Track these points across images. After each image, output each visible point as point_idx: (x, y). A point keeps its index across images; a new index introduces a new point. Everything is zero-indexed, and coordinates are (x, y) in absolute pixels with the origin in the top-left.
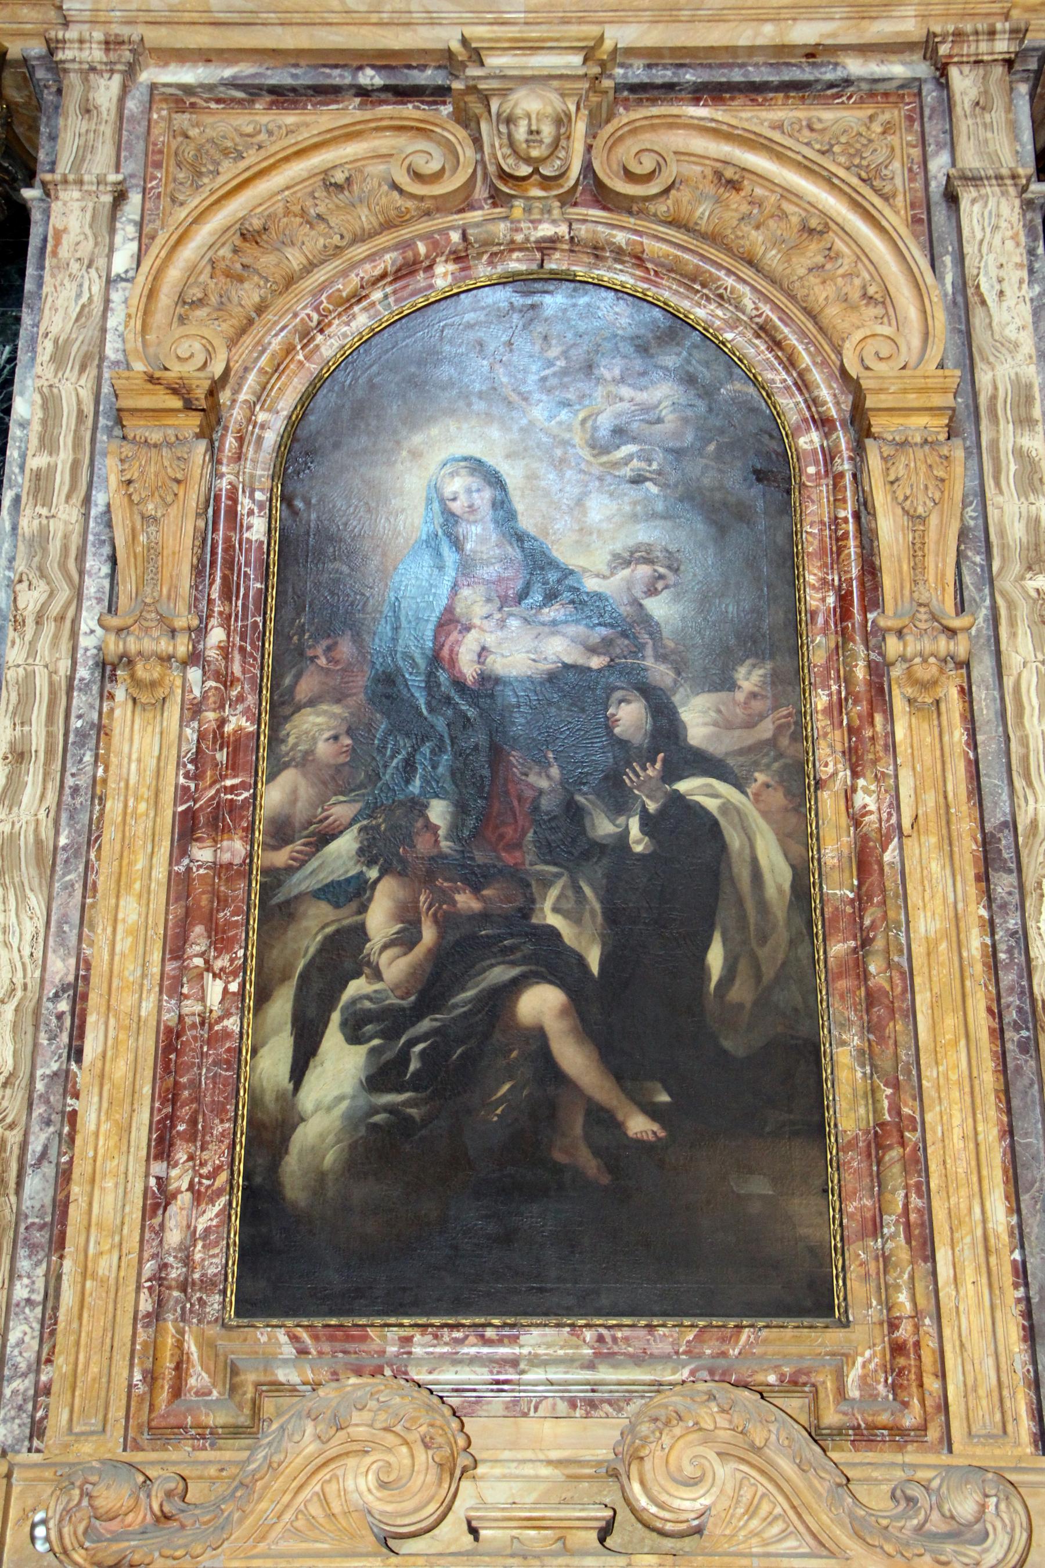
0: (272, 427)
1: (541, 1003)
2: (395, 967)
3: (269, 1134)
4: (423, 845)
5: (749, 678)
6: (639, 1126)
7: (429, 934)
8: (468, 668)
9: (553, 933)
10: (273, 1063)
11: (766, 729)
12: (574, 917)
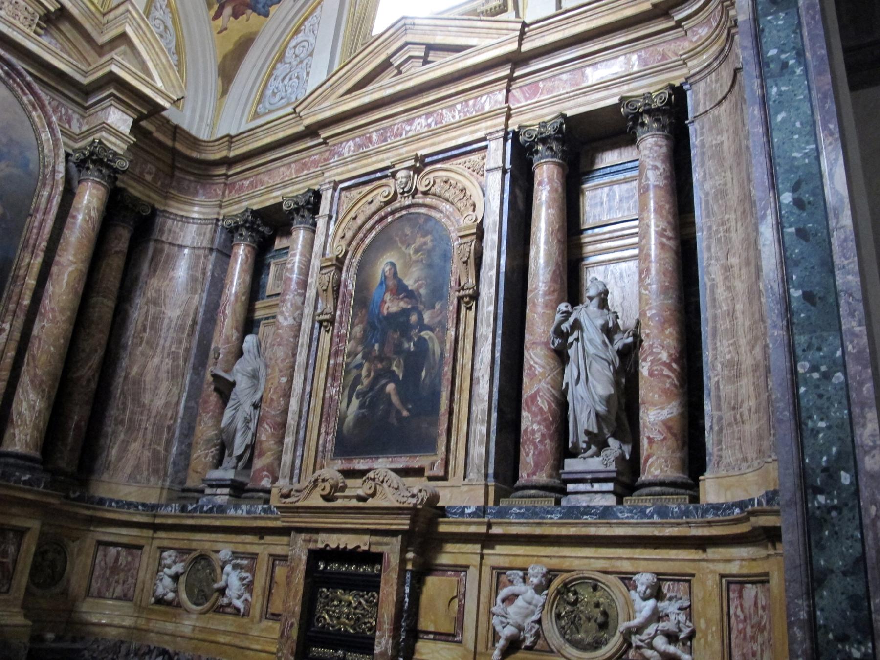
1: (390, 387)
2: (366, 382)
3: (342, 420)
4: (373, 354)
5: (438, 306)
6: (405, 413)
8: (385, 312)
9: (394, 371)
11: (439, 318)
12: (398, 366)
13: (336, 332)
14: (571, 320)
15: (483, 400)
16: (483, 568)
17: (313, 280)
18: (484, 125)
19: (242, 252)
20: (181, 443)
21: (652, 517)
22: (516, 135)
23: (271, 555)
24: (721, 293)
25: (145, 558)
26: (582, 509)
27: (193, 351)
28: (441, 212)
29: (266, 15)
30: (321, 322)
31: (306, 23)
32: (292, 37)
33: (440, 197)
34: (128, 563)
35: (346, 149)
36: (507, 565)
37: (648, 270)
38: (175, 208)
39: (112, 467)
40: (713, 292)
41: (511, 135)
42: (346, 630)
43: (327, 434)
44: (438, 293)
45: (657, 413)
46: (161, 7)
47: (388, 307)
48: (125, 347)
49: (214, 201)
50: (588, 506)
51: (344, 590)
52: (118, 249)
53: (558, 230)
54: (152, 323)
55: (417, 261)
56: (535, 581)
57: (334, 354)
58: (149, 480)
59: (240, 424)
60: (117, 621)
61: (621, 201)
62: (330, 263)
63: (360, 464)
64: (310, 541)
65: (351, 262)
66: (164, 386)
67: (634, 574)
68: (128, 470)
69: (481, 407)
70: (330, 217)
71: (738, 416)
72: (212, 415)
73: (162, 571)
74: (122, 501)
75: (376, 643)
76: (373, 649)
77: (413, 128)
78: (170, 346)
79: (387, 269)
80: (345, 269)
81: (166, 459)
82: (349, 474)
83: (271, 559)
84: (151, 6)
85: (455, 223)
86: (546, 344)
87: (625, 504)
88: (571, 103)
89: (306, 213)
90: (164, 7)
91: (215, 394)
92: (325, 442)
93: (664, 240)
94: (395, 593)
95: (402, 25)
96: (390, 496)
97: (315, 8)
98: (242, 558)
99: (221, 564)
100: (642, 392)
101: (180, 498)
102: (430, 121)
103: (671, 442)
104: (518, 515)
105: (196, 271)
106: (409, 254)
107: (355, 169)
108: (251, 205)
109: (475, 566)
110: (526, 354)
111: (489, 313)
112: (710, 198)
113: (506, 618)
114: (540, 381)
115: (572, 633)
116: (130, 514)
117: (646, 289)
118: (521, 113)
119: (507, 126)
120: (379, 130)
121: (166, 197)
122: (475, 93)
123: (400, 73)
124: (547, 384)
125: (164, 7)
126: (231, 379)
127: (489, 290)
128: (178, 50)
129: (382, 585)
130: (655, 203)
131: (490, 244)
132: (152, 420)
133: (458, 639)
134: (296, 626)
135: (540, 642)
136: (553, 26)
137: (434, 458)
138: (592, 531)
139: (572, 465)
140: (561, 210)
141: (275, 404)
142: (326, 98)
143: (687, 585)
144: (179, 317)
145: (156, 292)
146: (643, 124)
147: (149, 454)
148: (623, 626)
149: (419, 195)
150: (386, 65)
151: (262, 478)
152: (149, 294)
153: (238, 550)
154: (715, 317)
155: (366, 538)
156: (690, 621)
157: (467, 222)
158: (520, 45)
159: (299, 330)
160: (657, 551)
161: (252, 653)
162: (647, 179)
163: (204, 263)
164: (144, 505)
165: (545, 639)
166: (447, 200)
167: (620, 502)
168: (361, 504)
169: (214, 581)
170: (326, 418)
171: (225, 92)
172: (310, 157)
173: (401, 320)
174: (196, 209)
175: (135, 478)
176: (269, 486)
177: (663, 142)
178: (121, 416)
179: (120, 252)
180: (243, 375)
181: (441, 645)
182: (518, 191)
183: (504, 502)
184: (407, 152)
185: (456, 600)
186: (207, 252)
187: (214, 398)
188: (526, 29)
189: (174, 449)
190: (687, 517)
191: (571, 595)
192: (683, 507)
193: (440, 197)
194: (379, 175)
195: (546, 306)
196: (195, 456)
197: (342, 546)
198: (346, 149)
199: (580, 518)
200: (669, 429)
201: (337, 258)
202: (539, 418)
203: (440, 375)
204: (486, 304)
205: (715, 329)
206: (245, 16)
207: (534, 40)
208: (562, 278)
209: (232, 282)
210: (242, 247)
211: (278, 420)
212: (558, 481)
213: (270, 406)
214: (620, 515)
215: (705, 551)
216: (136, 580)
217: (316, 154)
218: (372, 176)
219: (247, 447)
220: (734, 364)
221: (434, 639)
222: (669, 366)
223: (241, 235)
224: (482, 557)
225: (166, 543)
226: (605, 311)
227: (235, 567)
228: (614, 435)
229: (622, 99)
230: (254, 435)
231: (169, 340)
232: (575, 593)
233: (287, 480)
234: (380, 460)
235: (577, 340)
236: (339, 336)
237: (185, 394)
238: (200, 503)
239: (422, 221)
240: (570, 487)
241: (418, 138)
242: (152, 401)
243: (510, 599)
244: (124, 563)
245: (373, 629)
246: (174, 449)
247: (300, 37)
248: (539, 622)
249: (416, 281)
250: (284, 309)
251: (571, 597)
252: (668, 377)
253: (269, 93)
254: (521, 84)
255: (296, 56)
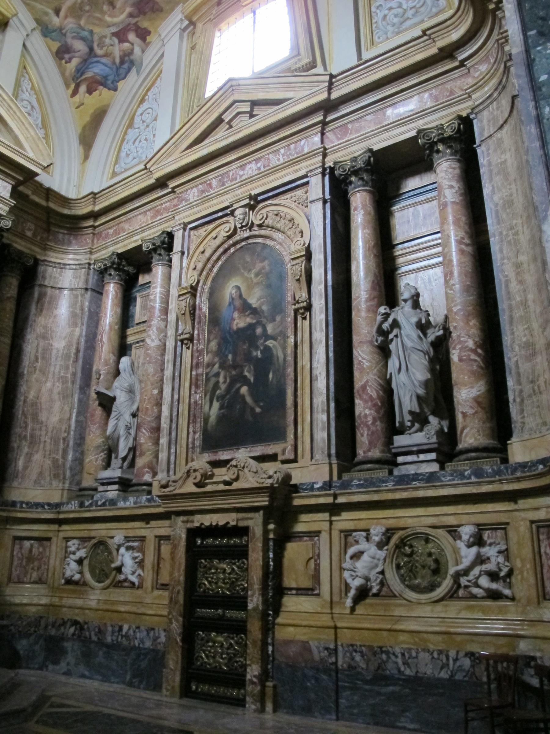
0: (207, 288)
1: (244, 390)
2: (223, 387)
3: (206, 420)
4: (228, 363)
5: (278, 318)
6: (258, 410)
7: (228, 380)
9: (246, 376)
10: (207, 408)
11: (280, 329)
12: (249, 372)
13: (195, 347)
14: (390, 320)
15: (321, 394)
16: (333, 532)
17: (173, 307)
18: (304, 164)
19: (112, 290)
20: (75, 451)
21: (469, 478)
22: (332, 169)
23: (156, 537)
24: (514, 286)
25: (54, 548)
26: (411, 477)
27: (79, 375)
28: (274, 240)
29: (115, 90)
30: (182, 341)
31: (149, 93)
32: (138, 106)
33: (272, 228)
34: (40, 553)
35: (191, 195)
36: (352, 528)
37: (452, 273)
38: (53, 257)
39: (20, 475)
40: (507, 286)
41: (328, 171)
42: (223, 593)
43: (195, 432)
44: (277, 308)
45: (467, 392)
46: (27, 91)
47: (237, 323)
48: (22, 375)
49: (86, 249)
50: (416, 474)
51: (220, 560)
52: (9, 295)
53: (374, 246)
54: (43, 354)
55: (258, 283)
56: (377, 539)
57: (195, 366)
58: (51, 484)
59: (122, 431)
60: (35, 601)
61: (424, 218)
62: (185, 291)
63: (224, 455)
64: (187, 522)
65: (203, 288)
66: (57, 406)
67: (459, 526)
68: (34, 477)
69: (320, 399)
70: (183, 253)
71: (536, 388)
72: (99, 426)
73: (68, 557)
74: (31, 503)
75: (249, 601)
76: (246, 606)
77: (246, 172)
78: (60, 372)
79: (234, 292)
80: (198, 295)
81: (64, 465)
82: (216, 464)
83: (157, 539)
84: (18, 90)
85: (287, 249)
86: (371, 342)
87: (447, 469)
88: (376, 139)
89: (163, 252)
90: (29, 90)
91: (100, 408)
92: (194, 440)
93: (463, 247)
94: (261, 558)
95: (231, 86)
96: (251, 479)
97: (156, 79)
98: (133, 541)
99: (116, 547)
100: (454, 375)
101: (78, 496)
102: (259, 165)
103: (482, 415)
104: (359, 486)
105: (75, 308)
106: (251, 278)
107: (200, 211)
108: (116, 249)
109: (325, 531)
110: (355, 352)
111: (321, 321)
112: (499, 208)
113: (355, 572)
114: (368, 373)
115: (410, 579)
116: (39, 512)
117: (451, 289)
118: (335, 152)
119: (324, 163)
120: (217, 177)
121: (45, 248)
122: (295, 138)
123: (231, 127)
124: (374, 375)
125: (29, 90)
126: (111, 394)
127: (320, 301)
128: (44, 126)
129: (250, 553)
130: (454, 217)
131: (317, 263)
132: (49, 434)
133: (316, 592)
134: (182, 593)
135: (385, 589)
136: (356, 75)
137: (283, 446)
138: (421, 494)
139: (400, 441)
140: (375, 230)
141: (150, 412)
142: (170, 155)
143: (503, 532)
144: (64, 347)
145: (43, 328)
146: (438, 151)
147: (49, 462)
148: (452, 570)
149: (256, 228)
150: (219, 121)
151: (143, 475)
152: (38, 330)
153: (130, 535)
154: (511, 308)
155: (234, 515)
156: (508, 561)
157: (296, 247)
158: (329, 94)
159: (164, 350)
160: (476, 506)
161: (147, 618)
162: (445, 197)
163: (81, 301)
164: (49, 504)
165: (389, 587)
166: (279, 230)
167: (442, 468)
168: (228, 488)
169: (112, 562)
170: (193, 420)
171: (86, 157)
172: (162, 204)
173: (249, 332)
174: (71, 256)
175: (40, 483)
176: (150, 480)
177: (456, 165)
178: (24, 433)
179: (12, 297)
180: (122, 390)
181: (302, 598)
182: (338, 218)
183: (346, 477)
184: (242, 193)
185: (312, 561)
186: (83, 291)
187: (99, 411)
188: (334, 80)
189: (70, 457)
190: (500, 476)
191: (407, 548)
192: (495, 468)
193: (272, 228)
194: (220, 214)
195: (368, 310)
196: (87, 460)
197: (214, 524)
198: (191, 195)
199: (410, 484)
200: (479, 404)
201: (192, 287)
202: (370, 404)
203: (284, 376)
204: (318, 313)
205: (511, 318)
206: (97, 91)
207: (340, 88)
208: (380, 287)
209: (106, 315)
210: (112, 285)
211: (154, 425)
212: (389, 455)
213: (146, 414)
214: (443, 479)
215: (516, 503)
216: (48, 566)
217: (167, 202)
218: (215, 216)
219: (130, 449)
220: (529, 345)
221: (297, 594)
222: (474, 351)
223: (110, 275)
224: (331, 522)
225: (70, 534)
226: (418, 310)
227: (128, 548)
228: (434, 414)
229: (419, 132)
230: (135, 439)
231: (58, 367)
232: (411, 546)
233: (165, 473)
234: (240, 451)
235: (396, 336)
236: (198, 351)
237: (75, 411)
238: (95, 499)
239: (259, 249)
240: (400, 459)
241: (251, 180)
242: (48, 418)
243: (357, 556)
244: (37, 553)
245: (245, 589)
246: (70, 457)
247: (145, 105)
248: (382, 572)
249: (258, 300)
250: (151, 333)
251: (408, 550)
252: (475, 361)
253: (123, 154)
254: (333, 127)
255: (144, 122)
